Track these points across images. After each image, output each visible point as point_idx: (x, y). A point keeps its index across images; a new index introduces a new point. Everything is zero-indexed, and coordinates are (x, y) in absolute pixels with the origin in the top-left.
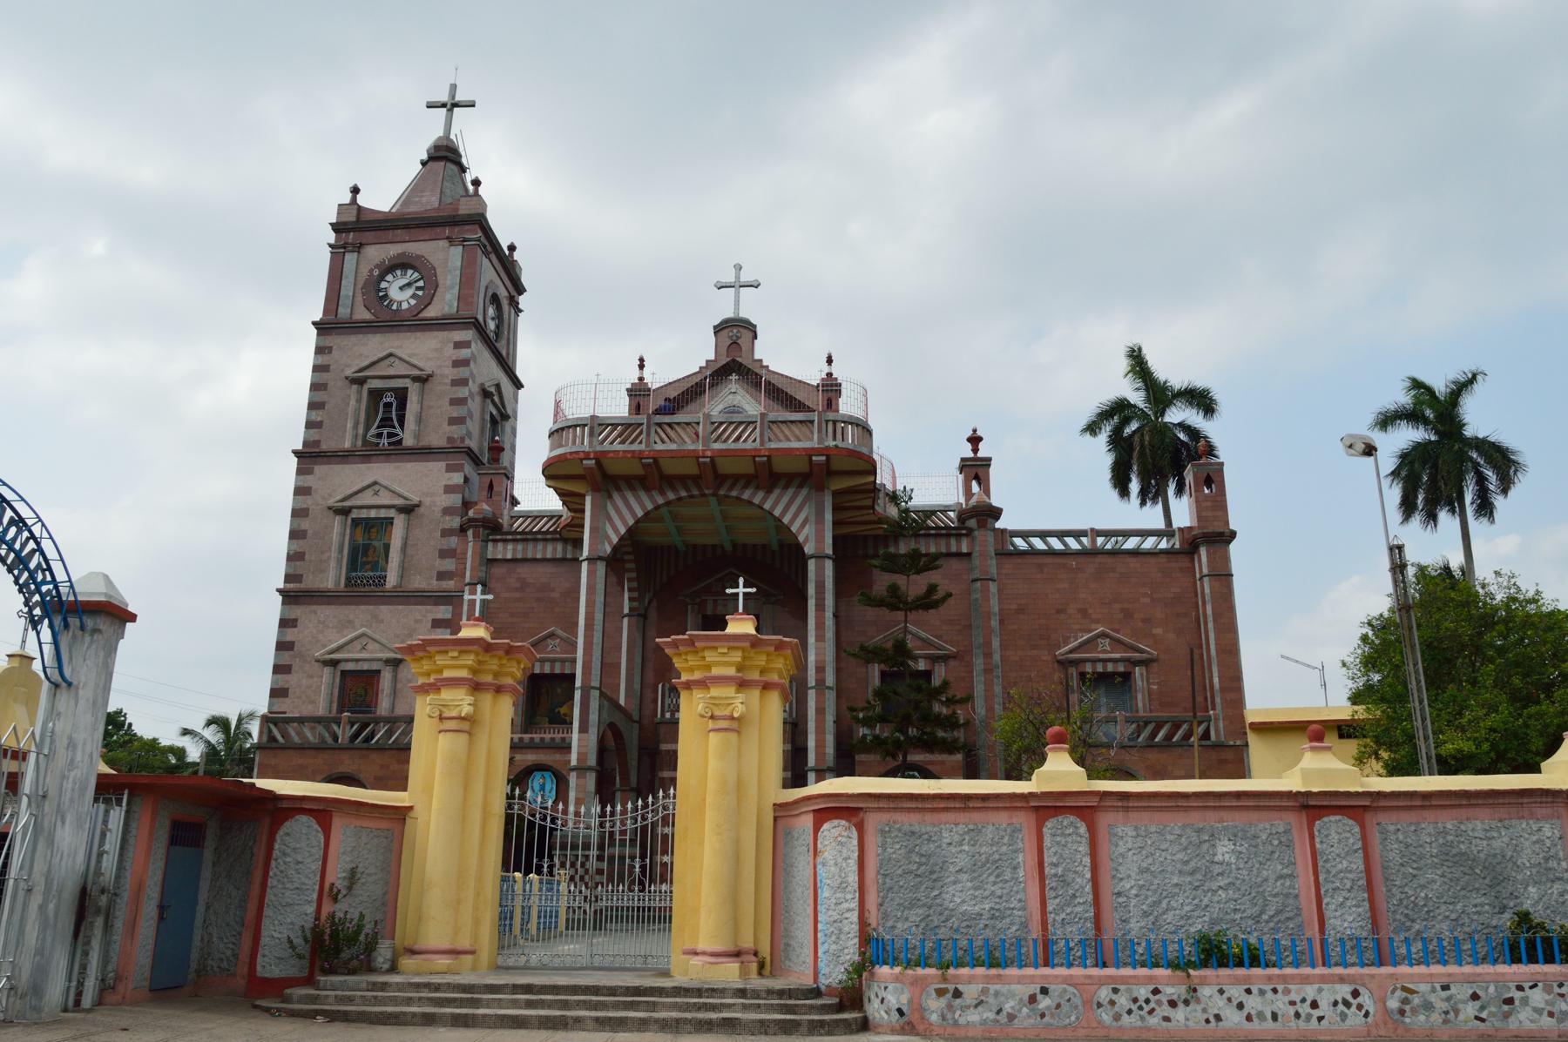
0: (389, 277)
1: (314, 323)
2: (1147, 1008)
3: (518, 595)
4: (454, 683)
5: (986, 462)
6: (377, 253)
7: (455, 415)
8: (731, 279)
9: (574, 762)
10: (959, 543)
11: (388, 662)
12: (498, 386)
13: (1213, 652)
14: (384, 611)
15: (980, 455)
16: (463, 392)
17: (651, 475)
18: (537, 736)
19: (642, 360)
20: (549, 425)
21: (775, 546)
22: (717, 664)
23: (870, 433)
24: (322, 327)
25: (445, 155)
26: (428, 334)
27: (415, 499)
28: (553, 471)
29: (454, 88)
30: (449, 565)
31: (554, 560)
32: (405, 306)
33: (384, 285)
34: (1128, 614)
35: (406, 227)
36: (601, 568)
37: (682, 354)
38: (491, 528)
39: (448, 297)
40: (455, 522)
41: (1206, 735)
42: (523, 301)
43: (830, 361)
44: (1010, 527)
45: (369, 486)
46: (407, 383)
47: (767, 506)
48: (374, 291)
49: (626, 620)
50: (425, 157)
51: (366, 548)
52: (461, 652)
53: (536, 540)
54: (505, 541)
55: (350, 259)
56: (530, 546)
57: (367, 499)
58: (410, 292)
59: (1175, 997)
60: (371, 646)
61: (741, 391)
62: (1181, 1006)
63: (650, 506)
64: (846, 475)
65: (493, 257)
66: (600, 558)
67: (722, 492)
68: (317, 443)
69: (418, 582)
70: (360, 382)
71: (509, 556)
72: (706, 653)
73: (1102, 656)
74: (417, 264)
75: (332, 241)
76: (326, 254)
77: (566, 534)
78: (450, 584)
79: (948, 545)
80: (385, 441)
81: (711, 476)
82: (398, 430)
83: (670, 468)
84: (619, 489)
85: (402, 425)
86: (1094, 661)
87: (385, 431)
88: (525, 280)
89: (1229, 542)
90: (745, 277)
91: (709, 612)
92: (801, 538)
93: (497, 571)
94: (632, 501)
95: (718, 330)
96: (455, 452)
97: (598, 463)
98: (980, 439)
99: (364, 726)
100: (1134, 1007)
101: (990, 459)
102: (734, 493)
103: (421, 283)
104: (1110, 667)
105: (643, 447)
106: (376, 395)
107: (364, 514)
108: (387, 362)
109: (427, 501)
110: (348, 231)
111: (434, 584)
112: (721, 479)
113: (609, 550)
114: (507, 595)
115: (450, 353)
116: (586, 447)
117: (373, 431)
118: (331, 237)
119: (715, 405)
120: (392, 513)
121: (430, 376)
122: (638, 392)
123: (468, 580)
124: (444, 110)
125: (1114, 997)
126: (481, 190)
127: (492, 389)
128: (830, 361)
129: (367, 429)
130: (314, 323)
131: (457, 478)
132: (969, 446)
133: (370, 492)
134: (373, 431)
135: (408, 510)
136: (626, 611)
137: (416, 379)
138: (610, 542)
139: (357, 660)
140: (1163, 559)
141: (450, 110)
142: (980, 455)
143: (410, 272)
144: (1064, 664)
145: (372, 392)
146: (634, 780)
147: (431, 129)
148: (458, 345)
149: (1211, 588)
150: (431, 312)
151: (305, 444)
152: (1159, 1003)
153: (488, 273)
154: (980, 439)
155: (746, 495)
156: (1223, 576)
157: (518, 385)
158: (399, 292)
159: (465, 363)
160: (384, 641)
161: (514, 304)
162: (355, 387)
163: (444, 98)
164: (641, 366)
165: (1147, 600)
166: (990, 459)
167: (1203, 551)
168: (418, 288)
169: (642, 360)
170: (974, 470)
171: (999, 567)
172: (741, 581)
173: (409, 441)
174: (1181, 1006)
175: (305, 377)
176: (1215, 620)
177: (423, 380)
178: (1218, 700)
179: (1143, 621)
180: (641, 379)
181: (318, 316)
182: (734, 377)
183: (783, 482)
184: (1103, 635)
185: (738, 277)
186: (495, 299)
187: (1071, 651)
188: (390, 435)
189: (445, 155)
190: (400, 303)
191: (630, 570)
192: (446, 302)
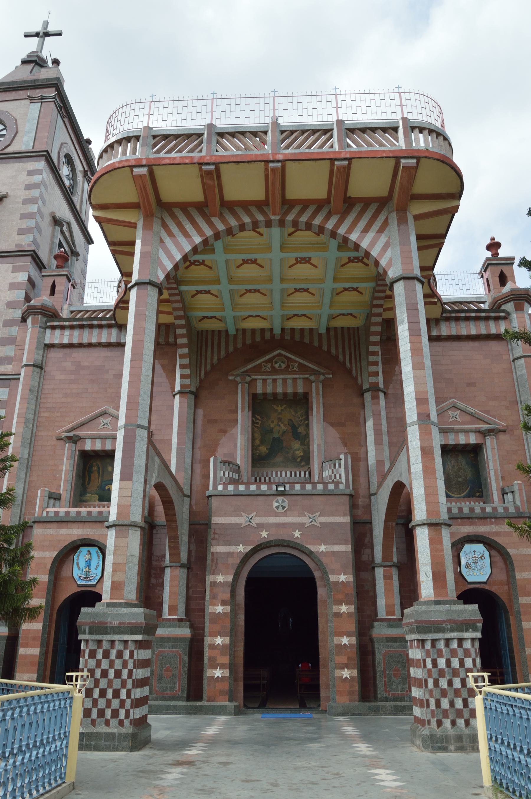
3: (73, 377)
7: (24, 226)
9: (113, 517)
18: (84, 510)
21: (323, 330)
26: (8, 163)
29: (46, 23)
36: (152, 294)
38: (50, 316)
39: (25, 139)
40: (18, 314)
49: (177, 397)
54: (63, 328)
56: (86, 331)
65: (66, 120)
66: (151, 283)
67: (290, 217)
71: (66, 341)
79: (488, 327)
91: (259, 390)
93: (54, 355)
94: (189, 227)
97: (151, 173)
105: (203, 154)
112: (289, 204)
113: (161, 276)
114: (62, 377)
115: (24, 179)
123: (24, 362)
136: (178, 388)
138: (163, 268)
146: (184, 556)
148: (30, 173)
150: (10, 149)
159: (36, 186)
163: (38, 28)
183: (358, 208)
191: (183, 346)
192: (24, 142)
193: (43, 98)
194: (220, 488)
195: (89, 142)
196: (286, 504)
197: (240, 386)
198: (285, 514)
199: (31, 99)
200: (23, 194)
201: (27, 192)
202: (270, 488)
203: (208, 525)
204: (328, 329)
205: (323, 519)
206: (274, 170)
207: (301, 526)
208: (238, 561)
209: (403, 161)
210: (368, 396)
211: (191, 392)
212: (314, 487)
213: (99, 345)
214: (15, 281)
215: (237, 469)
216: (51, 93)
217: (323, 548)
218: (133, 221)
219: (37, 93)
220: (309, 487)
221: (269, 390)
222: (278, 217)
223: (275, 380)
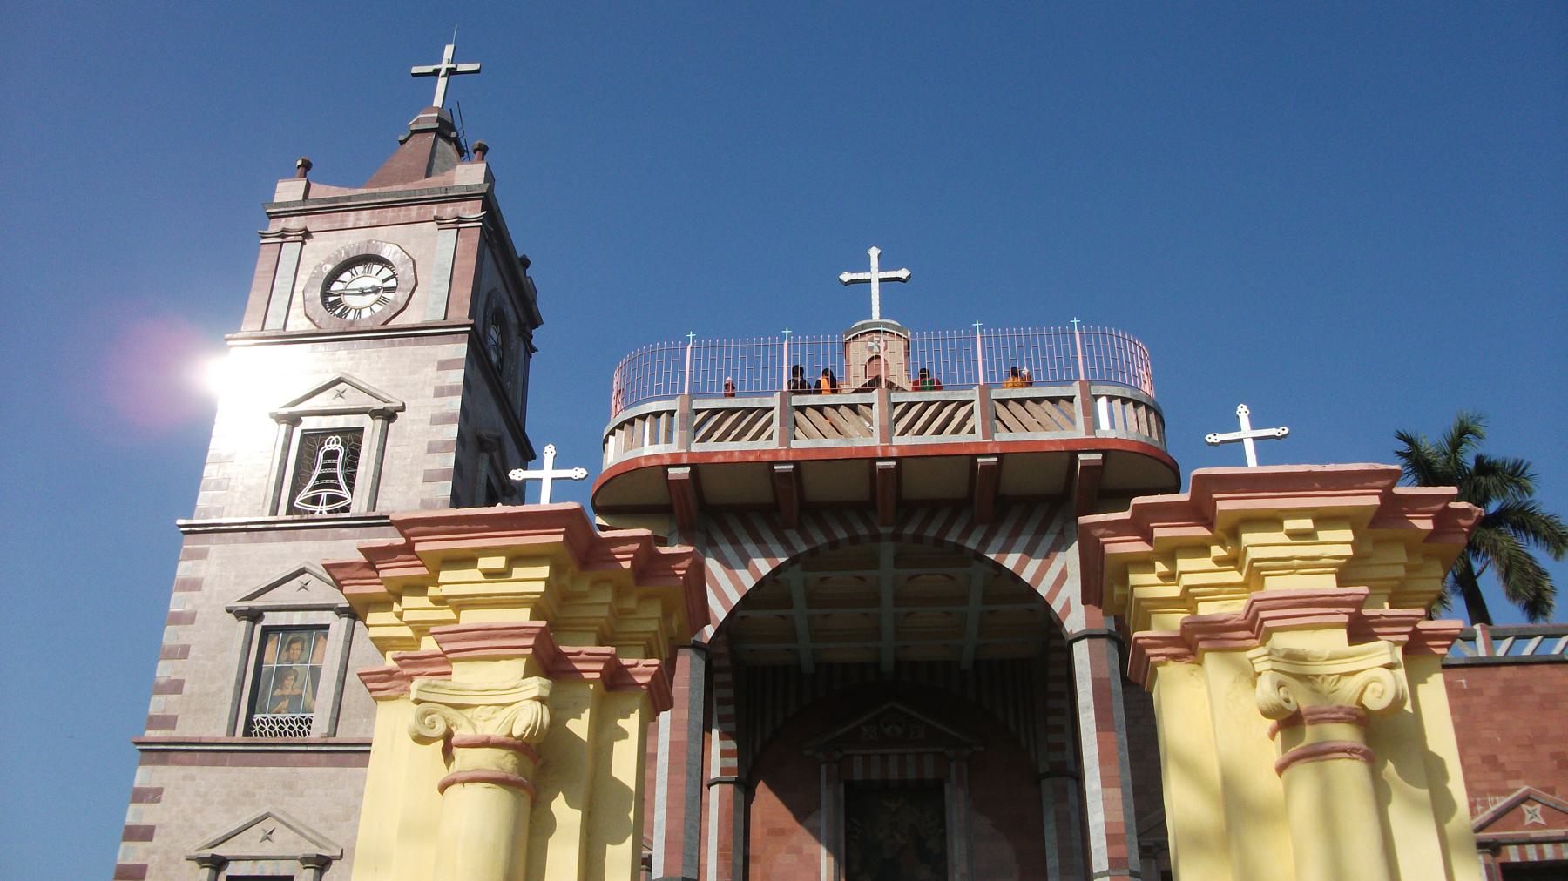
0: (346, 276)
11: (305, 861)
12: (499, 439)
22: (1286, 566)
32: (366, 314)
33: (336, 287)
46: (366, 421)
51: (281, 674)
72: (1247, 538)
73: (1534, 834)
80: (322, 510)
85: (351, 486)
86: (1521, 843)
87: (324, 494)
88: (542, 304)
91: (858, 775)
92: (1057, 606)
103: (392, 283)
106: (312, 440)
112: (906, 508)
117: (305, 493)
129: (295, 490)
136: (715, 773)
145: (306, 436)
161: (527, 339)
172: (1243, 413)
173: (358, 504)
177: (388, 416)
188: (332, 499)
190: (359, 311)
193: (461, 220)
195: (525, 263)
197: (823, 767)
206: (884, 471)
209: (1081, 457)
210: (1046, 784)
216: (473, 210)
219: (449, 210)
221: (875, 774)
222: (890, 530)
223: (884, 757)
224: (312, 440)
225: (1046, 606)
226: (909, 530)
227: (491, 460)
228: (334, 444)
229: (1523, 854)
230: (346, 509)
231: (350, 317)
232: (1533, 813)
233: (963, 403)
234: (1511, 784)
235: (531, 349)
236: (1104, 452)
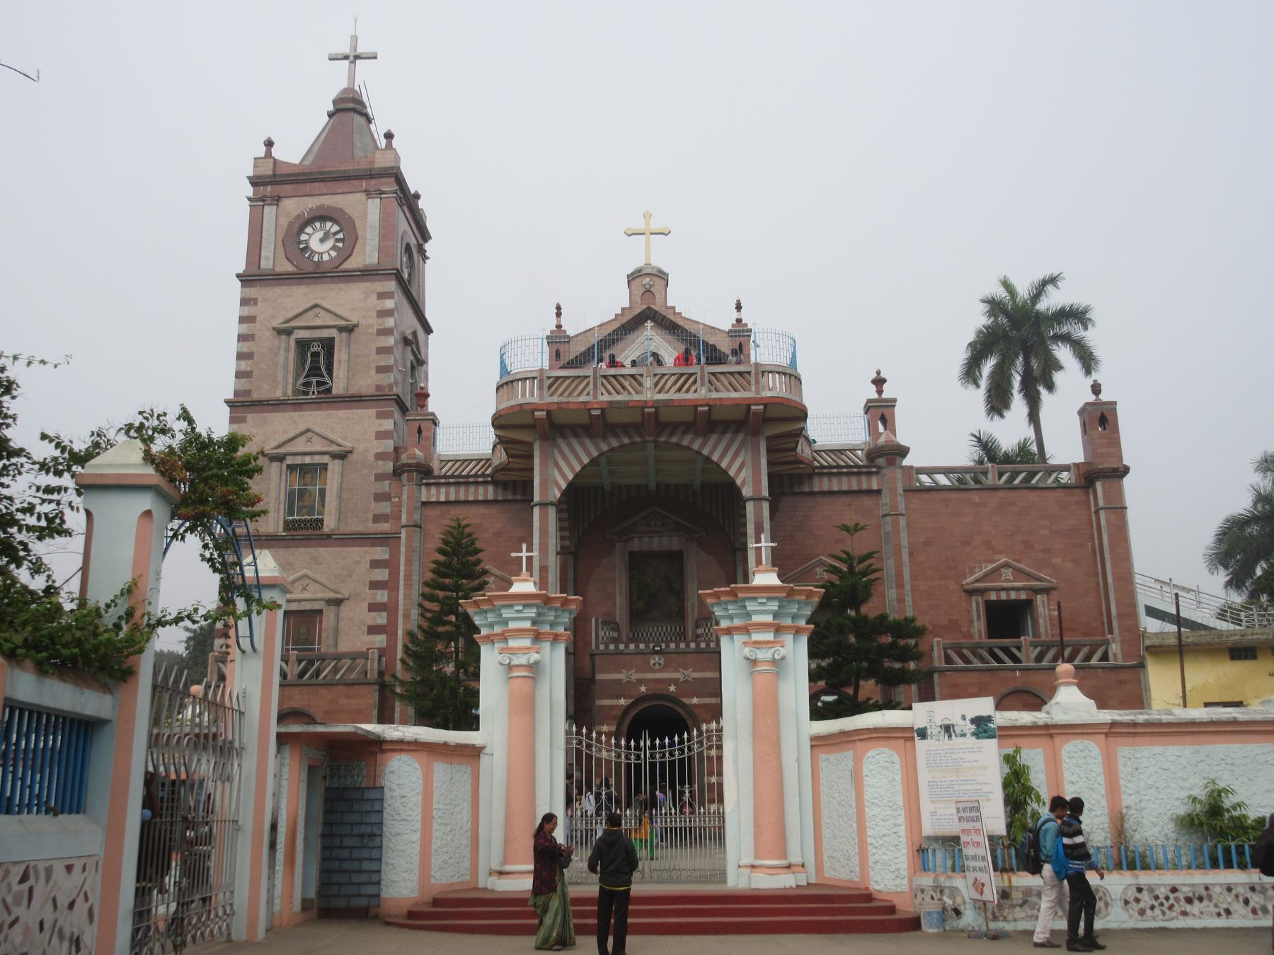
0: (309, 230)
1: (238, 276)
2: (1166, 905)
4: (520, 633)
5: (891, 403)
6: (295, 206)
7: (382, 363)
8: (640, 226)
10: (869, 481)
11: (329, 602)
12: (414, 333)
13: (1110, 580)
14: (324, 552)
15: (884, 396)
16: (391, 341)
17: (594, 425)
19: (558, 308)
20: (495, 378)
23: (800, 380)
24: (246, 279)
25: (350, 108)
27: (348, 445)
28: (503, 422)
29: (355, 39)
30: (385, 508)
31: (486, 502)
32: (326, 258)
33: (304, 237)
34: (1028, 546)
35: (323, 180)
36: (552, 512)
37: (597, 304)
38: (424, 472)
40: (389, 467)
41: (1105, 657)
42: (428, 246)
43: (739, 307)
44: (916, 464)
45: (302, 434)
47: (705, 452)
48: (292, 240)
50: (331, 108)
52: (525, 606)
53: (467, 483)
55: (270, 211)
57: (300, 446)
58: (330, 243)
59: (1190, 895)
60: (312, 587)
61: (658, 338)
62: (1196, 902)
63: (595, 453)
64: (779, 423)
68: (248, 392)
69: (355, 526)
70: (288, 332)
71: (443, 499)
73: (1006, 585)
74: (335, 216)
75: (251, 195)
76: (245, 208)
77: (499, 477)
78: (385, 527)
79: (860, 483)
80: (314, 389)
81: (654, 423)
82: (327, 379)
83: (614, 417)
84: (564, 437)
86: (998, 590)
88: (430, 225)
89: (1123, 476)
90: (655, 225)
92: (738, 482)
94: (578, 448)
95: (633, 277)
96: (376, 399)
98: (884, 381)
99: (311, 663)
100: (1156, 904)
101: (895, 400)
102: (674, 440)
103: (341, 236)
104: (1013, 595)
105: (590, 398)
106: (303, 345)
107: (298, 460)
108: (311, 313)
109: (360, 447)
110: (265, 184)
111: (372, 527)
113: (558, 495)
116: (536, 399)
118: (249, 190)
119: (629, 352)
120: (326, 459)
121: (356, 326)
122: (557, 341)
124: (347, 62)
125: (1138, 896)
126: (395, 142)
127: (410, 337)
128: (739, 307)
130: (238, 276)
131: (388, 425)
132: (874, 387)
133: (303, 438)
134: (301, 380)
135: (342, 456)
137: (341, 329)
138: (559, 487)
139: (299, 601)
140: (1060, 493)
141: (353, 62)
142: (884, 396)
143: (329, 224)
144: (971, 592)
147: (335, 81)
149: (1107, 520)
150: (353, 263)
151: (236, 393)
152: (1177, 900)
153: (403, 225)
154: (884, 381)
155: (685, 443)
156: (1119, 510)
157: (428, 330)
158: (319, 243)
159: (389, 313)
160: (327, 583)
161: (422, 252)
162: (283, 337)
163: (346, 50)
164: (559, 314)
165: (1046, 532)
166: (895, 400)
167: (1099, 486)
168: (338, 240)
169: (558, 308)
170: (880, 411)
171: (907, 503)
174: (1196, 902)
175: (233, 328)
176: (1111, 550)
177: (349, 329)
178: (1115, 624)
179: (1043, 551)
180: (559, 327)
181: (241, 269)
182: (649, 324)
184: (1006, 565)
185: (647, 224)
186: (408, 248)
187: (977, 581)
188: (319, 384)
189: (350, 108)
192: (367, 254)
194: (602, 647)
195: (417, 196)
196: (662, 661)
198: (660, 671)
199: (368, 193)
200: (375, 323)
201: (381, 321)
202: (647, 646)
203: (592, 680)
204: (703, 485)
205: (696, 675)
206: (649, 414)
207: (676, 682)
208: (620, 713)
211: (571, 553)
212: (688, 645)
213: (476, 502)
214: (382, 429)
215: (616, 628)
216: (390, 186)
217: (695, 701)
218: (530, 440)
220: (682, 645)
224: (303, 345)
225: (733, 482)
226: (662, 439)
227: (413, 351)
228: (315, 348)
229: (998, 596)
230: (329, 390)
231: (316, 259)
232: (1007, 573)
233: (691, 375)
234: (996, 557)
235: (425, 258)
236: (765, 405)
